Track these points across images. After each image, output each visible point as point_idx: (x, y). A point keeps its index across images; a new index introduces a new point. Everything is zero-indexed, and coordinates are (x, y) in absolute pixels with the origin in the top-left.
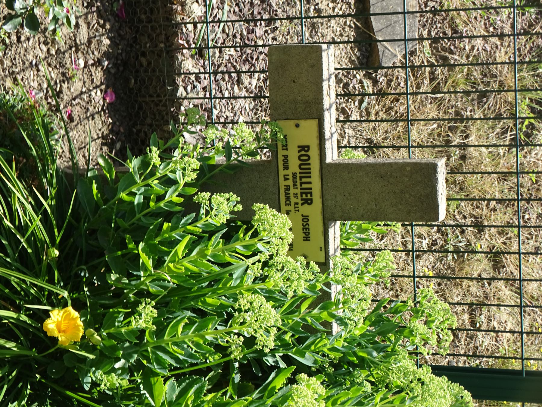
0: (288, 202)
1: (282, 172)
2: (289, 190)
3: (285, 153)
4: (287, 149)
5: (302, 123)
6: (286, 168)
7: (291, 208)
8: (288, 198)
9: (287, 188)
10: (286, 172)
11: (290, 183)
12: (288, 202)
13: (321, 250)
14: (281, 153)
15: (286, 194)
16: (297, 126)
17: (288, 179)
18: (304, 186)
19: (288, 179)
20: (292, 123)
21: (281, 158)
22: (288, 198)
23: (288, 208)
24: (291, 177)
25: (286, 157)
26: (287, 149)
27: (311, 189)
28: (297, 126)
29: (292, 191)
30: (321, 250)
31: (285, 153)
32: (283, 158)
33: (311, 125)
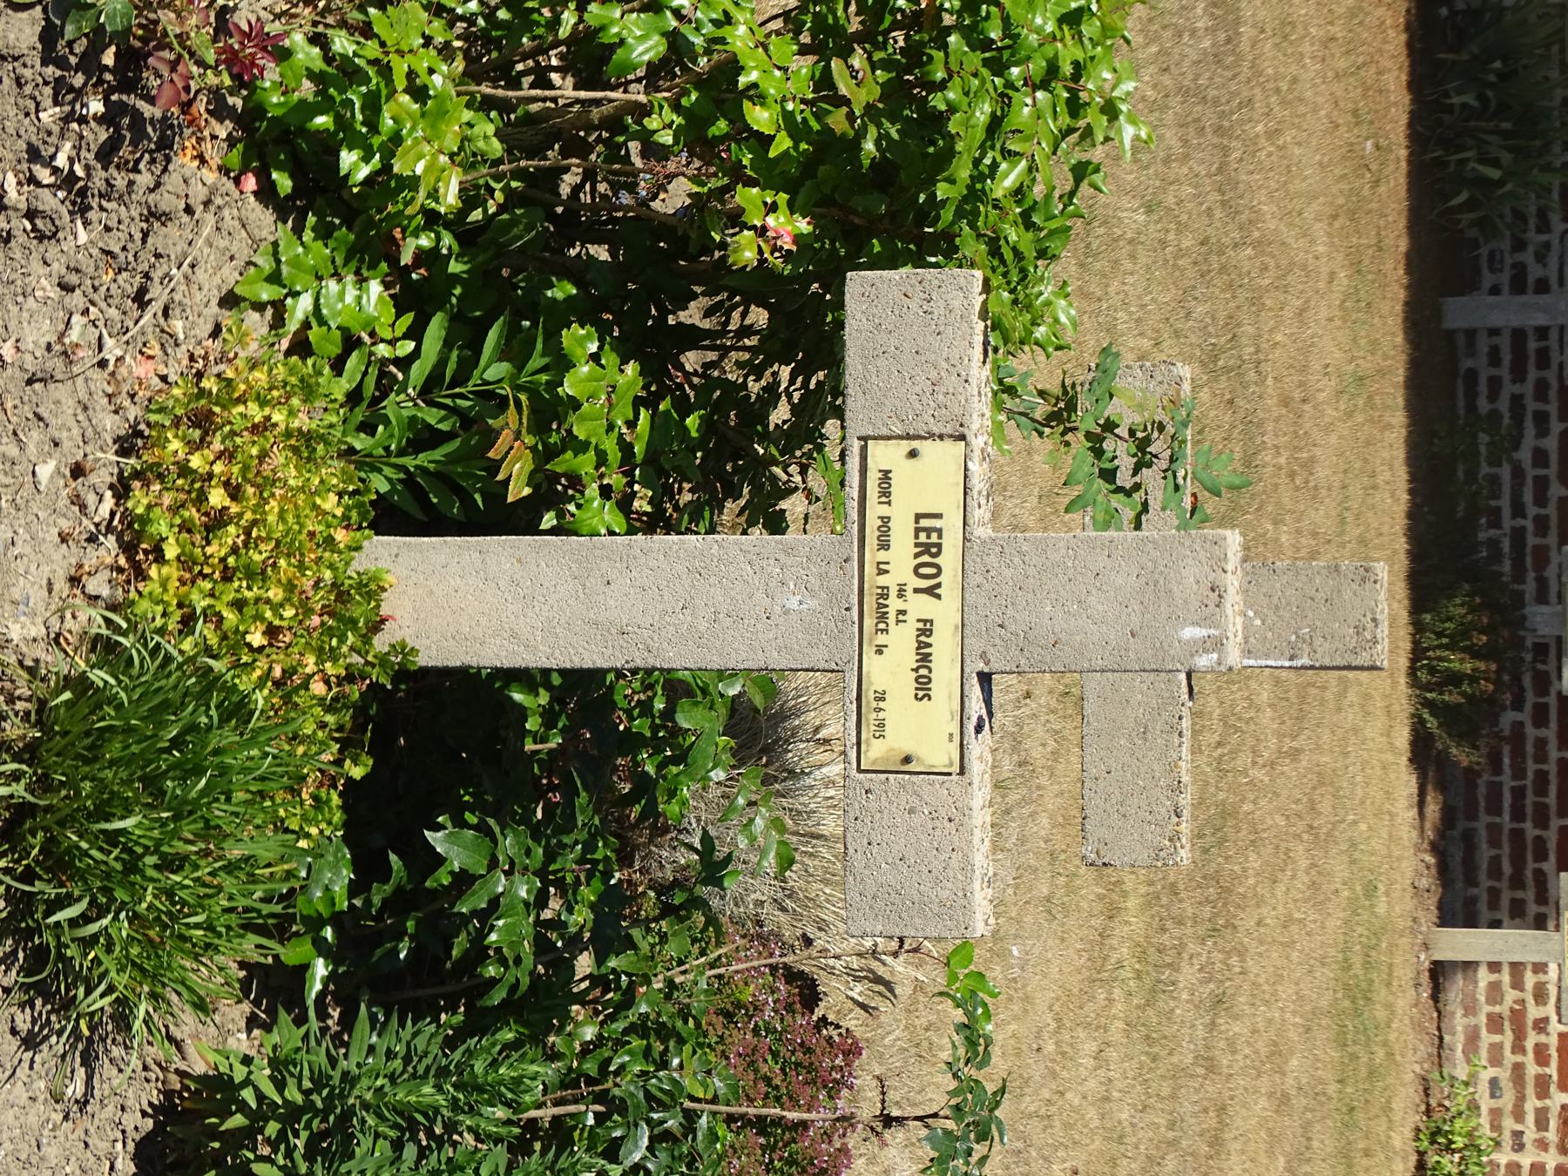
0: (882, 626)
2: (885, 596)
3: (884, 510)
4: (889, 503)
6: (884, 545)
8: (883, 617)
9: (884, 593)
10: (882, 556)
12: (882, 626)
14: (874, 511)
15: (881, 606)
20: (906, 446)
21: (872, 523)
23: (881, 639)
25: (885, 520)
26: (889, 503)
29: (894, 604)
31: (884, 510)
32: (879, 523)
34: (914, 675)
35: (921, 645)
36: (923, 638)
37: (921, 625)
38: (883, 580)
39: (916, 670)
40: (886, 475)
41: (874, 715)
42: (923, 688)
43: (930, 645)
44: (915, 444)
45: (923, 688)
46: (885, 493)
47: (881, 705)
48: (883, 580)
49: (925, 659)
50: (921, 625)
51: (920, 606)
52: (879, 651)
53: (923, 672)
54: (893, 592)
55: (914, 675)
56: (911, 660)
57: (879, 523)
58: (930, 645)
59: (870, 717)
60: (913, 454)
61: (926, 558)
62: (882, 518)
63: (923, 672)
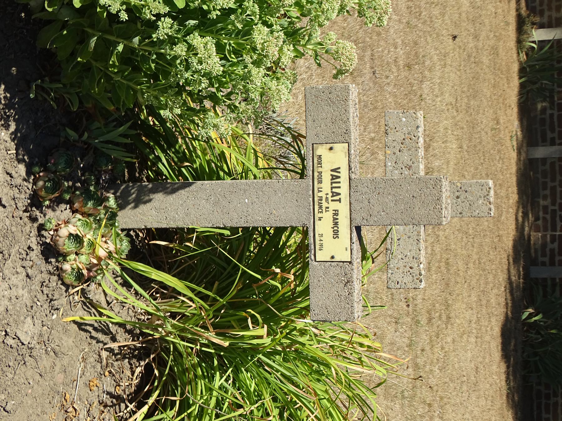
0: (320, 210)
4: (321, 167)
5: (335, 146)
6: (320, 182)
8: (321, 207)
9: (321, 199)
12: (320, 210)
13: (346, 250)
17: (321, 191)
18: (334, 190)
19: (321, 191)
26: (321, 167)
28: (331, 149)
30: (346, 250)
32: (318, 174)
33: (341, 148)
34: (332, 230)
35: (335, 219)
36: (335, 217)
37: (334, 212)
38: (320, 194)
39: (333, 228)
41: (319, 242)
42: (336, 234)
43: (338, 219)
44: (331, 145)
45: (336, 234)
46: (320, 163)
48: (320, 194)
49: (336, 224)
50: (334, 212)
51: (333, 206)
52: (320, 219)
53: (336, 228)
54: (324, 199)
55: (332, 230)
56: (331, 224)
58: (338, 219)
59: (318, 242)
62: (318, 172)
63: (336, 228)
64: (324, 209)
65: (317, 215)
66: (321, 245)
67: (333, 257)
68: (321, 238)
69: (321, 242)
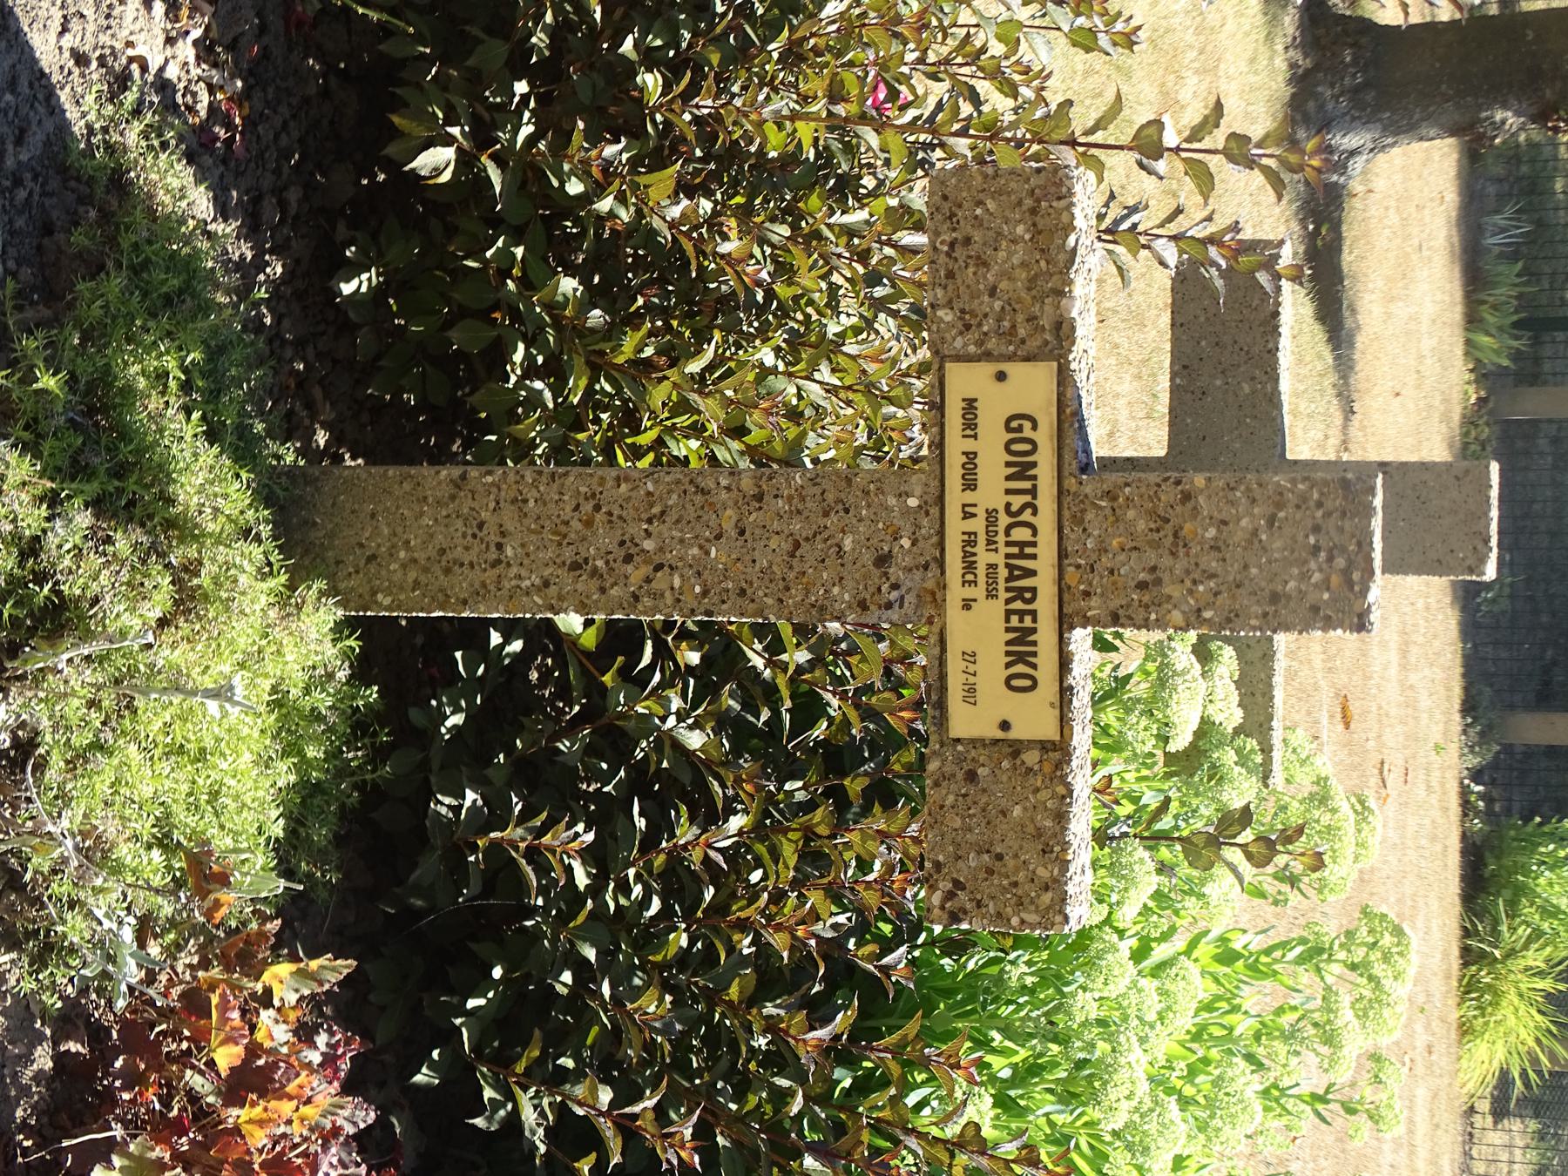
0: (969, 577)
1: (955, 496)
3: (970, 445)
4: (975, 437)
6: (970, 485)
7: (979, 592)
8: (970, 566)
10: (969, 497)
11: (978, 525)
12: (969, 577)
15: (966, 554)
16: (1001, 377)
22: (970, 566)
23: (969, 592)
24: (982, 515)
25: (971, 456)
26: (975, 437)
27: (1034, 557)
31: (970, 445)
32: (964, 459)
40: (970, 405)
47: (972, 668)
52: (967, 605)
57: (964, 459)
60: (1001, 377)
61: (1018, 605)
64: (981, 571)
65: (956, 592)
66: (971, 691)
67: (1005, 726)
68: (972, 668)
69: (972, 679)
